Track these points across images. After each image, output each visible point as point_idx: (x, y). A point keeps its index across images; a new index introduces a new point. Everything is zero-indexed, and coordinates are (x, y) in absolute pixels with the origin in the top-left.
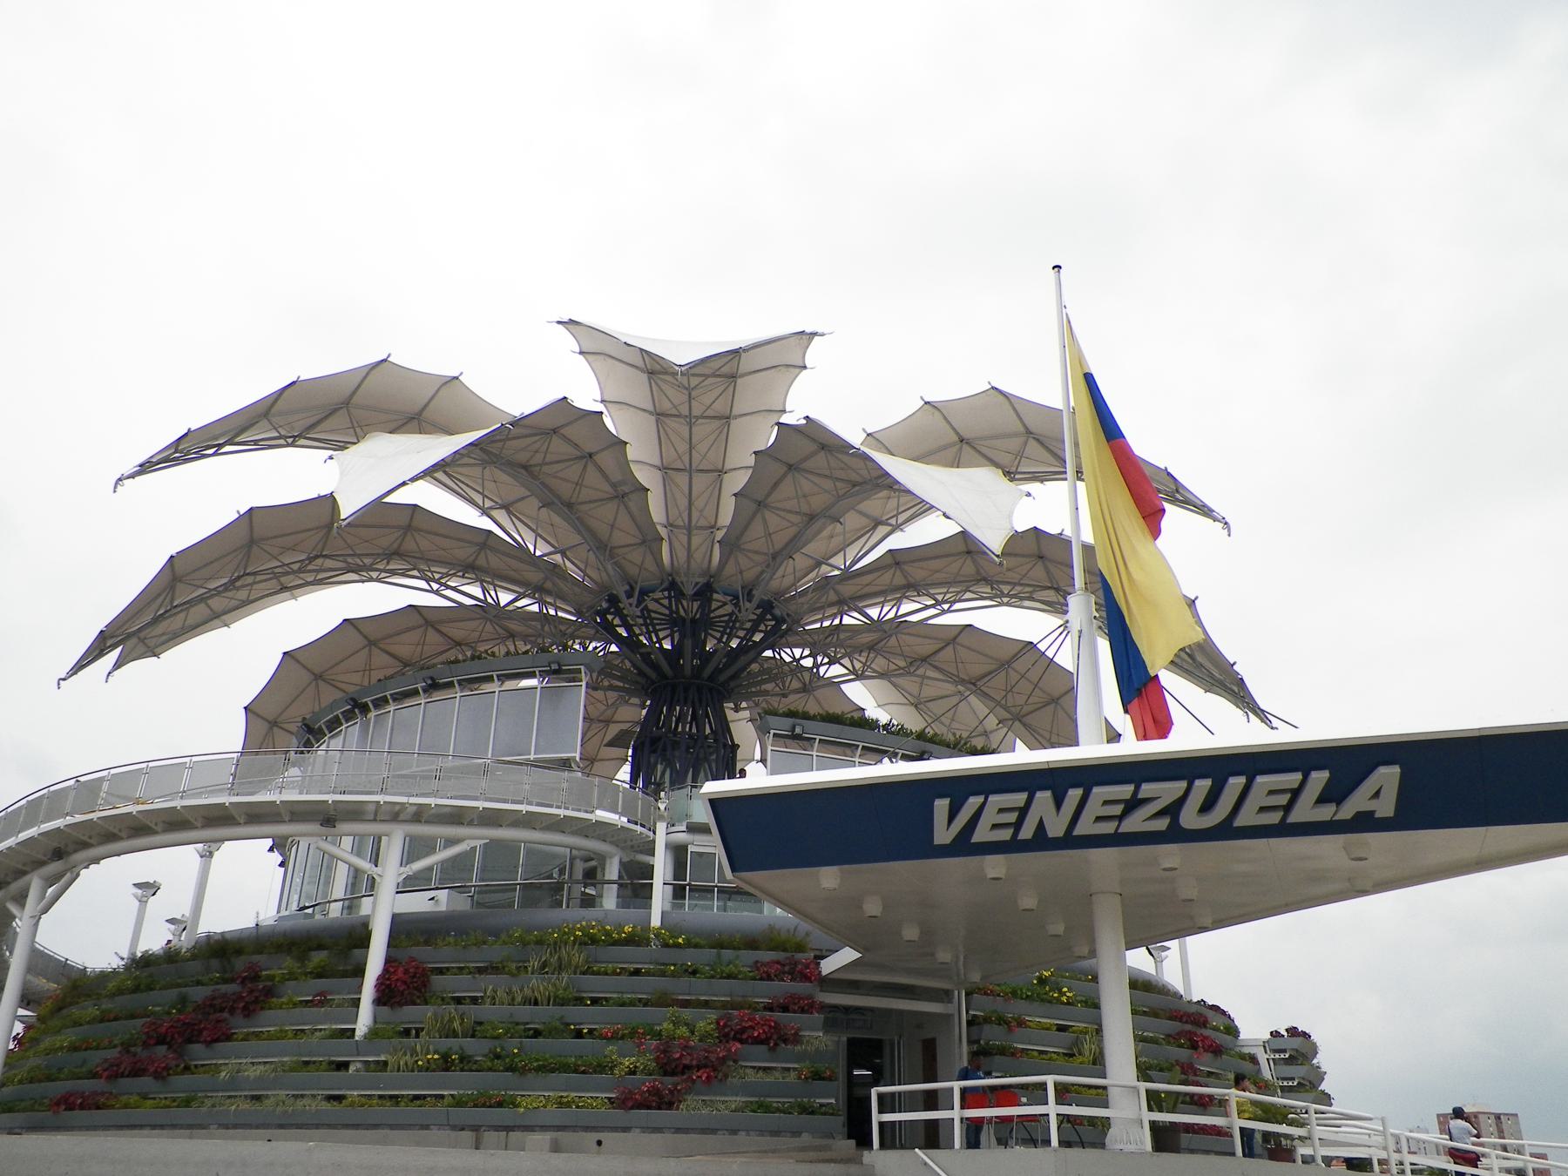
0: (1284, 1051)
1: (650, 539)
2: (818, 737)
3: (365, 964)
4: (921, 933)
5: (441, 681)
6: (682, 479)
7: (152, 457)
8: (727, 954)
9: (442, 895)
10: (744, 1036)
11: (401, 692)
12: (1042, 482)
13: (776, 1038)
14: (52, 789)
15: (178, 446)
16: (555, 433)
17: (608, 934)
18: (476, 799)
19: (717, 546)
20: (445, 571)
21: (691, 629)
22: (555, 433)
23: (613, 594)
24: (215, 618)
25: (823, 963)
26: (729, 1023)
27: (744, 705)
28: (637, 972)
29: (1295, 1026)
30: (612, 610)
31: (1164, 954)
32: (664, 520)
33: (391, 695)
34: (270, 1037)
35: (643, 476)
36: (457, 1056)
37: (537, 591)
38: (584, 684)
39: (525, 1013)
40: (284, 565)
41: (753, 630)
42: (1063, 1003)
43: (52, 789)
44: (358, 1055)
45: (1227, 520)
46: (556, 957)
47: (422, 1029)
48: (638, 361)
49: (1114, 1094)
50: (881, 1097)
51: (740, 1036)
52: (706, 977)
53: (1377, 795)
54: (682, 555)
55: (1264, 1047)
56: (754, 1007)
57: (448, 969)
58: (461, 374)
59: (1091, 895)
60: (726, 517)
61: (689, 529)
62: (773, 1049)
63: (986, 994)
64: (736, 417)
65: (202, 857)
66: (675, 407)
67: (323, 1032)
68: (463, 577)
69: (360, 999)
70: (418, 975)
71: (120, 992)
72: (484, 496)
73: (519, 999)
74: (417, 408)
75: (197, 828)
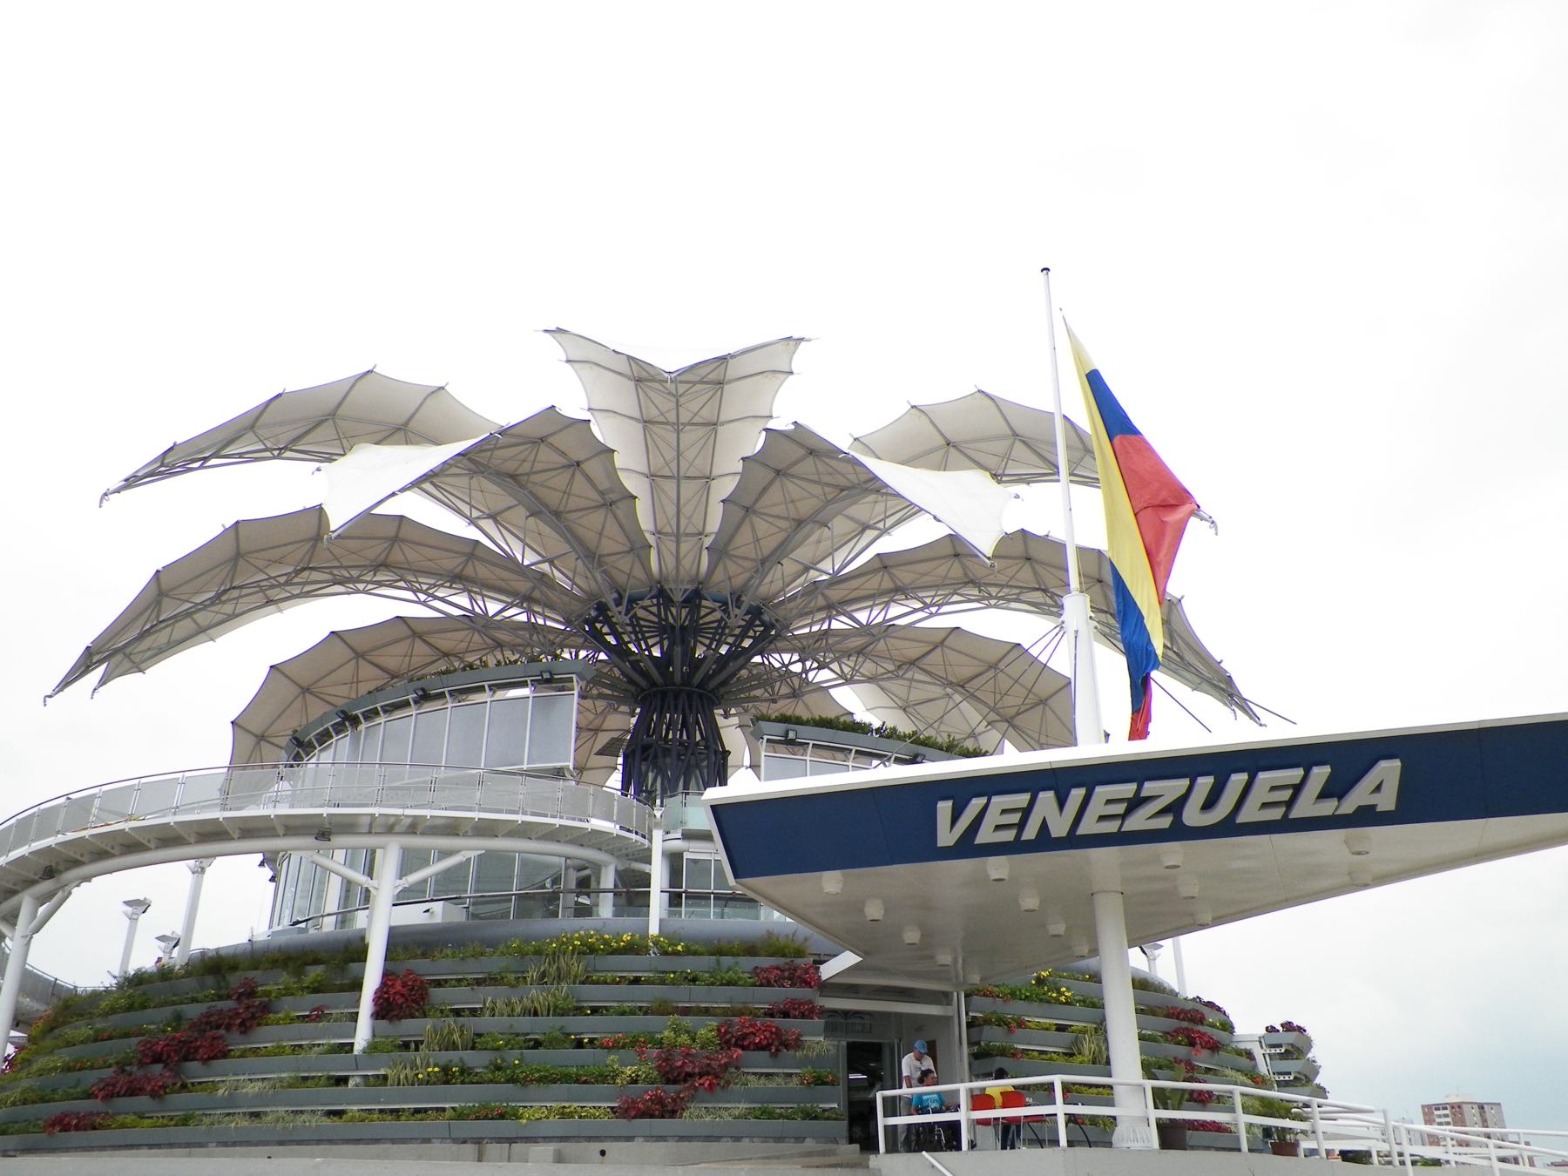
0: (1280, 1046)
1: (638, 548)
2: (811, 742)
3: (363, 978)
5: (432, 692)
6: (670, 487)
7: (137, 472)
8: (727, 961)
9: (437, 907)
10: (746, 1043)
11: (393, 703)
12: (1028, 484)
13: (777, 1044)
14: (42, 807)
15: (163, 460)
16: (543, 441)
17: (606, 943)
18: (471, 809)
19: (705, 553)
20: (432, 581)
21: (680, 636)
22: (543, 441)
23: (600, 602)
24: (201, 632)
25: (823, 968)
26: (730, 1030)
27: (733, 711)
28: (636, 981)
29: (1289, 1021)
30: (601, 618)
31: (1157, 952)
32: (652, 528)
33: (382, 707)
34: (268, 1053)
35: (632, 484)
36: (457, 1069)
37: (525, 600)
38: (576, 692)
39: (524, 1024)
40: (271, 578)
41: (743, 636)
42: (1062, 1003)
43: (42, 807)
44: (357, 1069)
45: (1214, 518)
46: (555, 967)
47: (422, 1042)
48: (625, 368)
49: (1119, 1092)
50: (885, 1099)
51: (742, 1042)
52: (708, 985)
53: (1378, 789)
54: (670, 562)
55: (1260, 1042)
56: (754, 1013)
57: (446, 981)
58: (447, 384)
59: (1092, 894)
60: (714, 523)
61: (678, 537)
62: (775, 1055)
63: (985, 995)
64: (723, 424)
65: (193, 873)
66: (662, 414)
67: (321, 1047)
68: (450, 587)
69: (358, 1013)
70: (416, 988)
71: (113, 1011)
72: (472, 506)
73: (518, 1010)
74: (401, 421)
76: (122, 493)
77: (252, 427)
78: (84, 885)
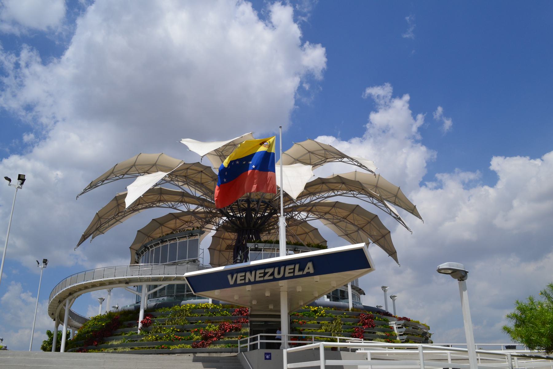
4: (257, 302)
7: (86, 188)
9: (165, 298)
24: (117, 221)
44: (138, 338)
53: (309, 268)
74: (154, 163)
75: (98, 286)
76: (82, 195)
77: (112, 172)
78: (79, 297)
